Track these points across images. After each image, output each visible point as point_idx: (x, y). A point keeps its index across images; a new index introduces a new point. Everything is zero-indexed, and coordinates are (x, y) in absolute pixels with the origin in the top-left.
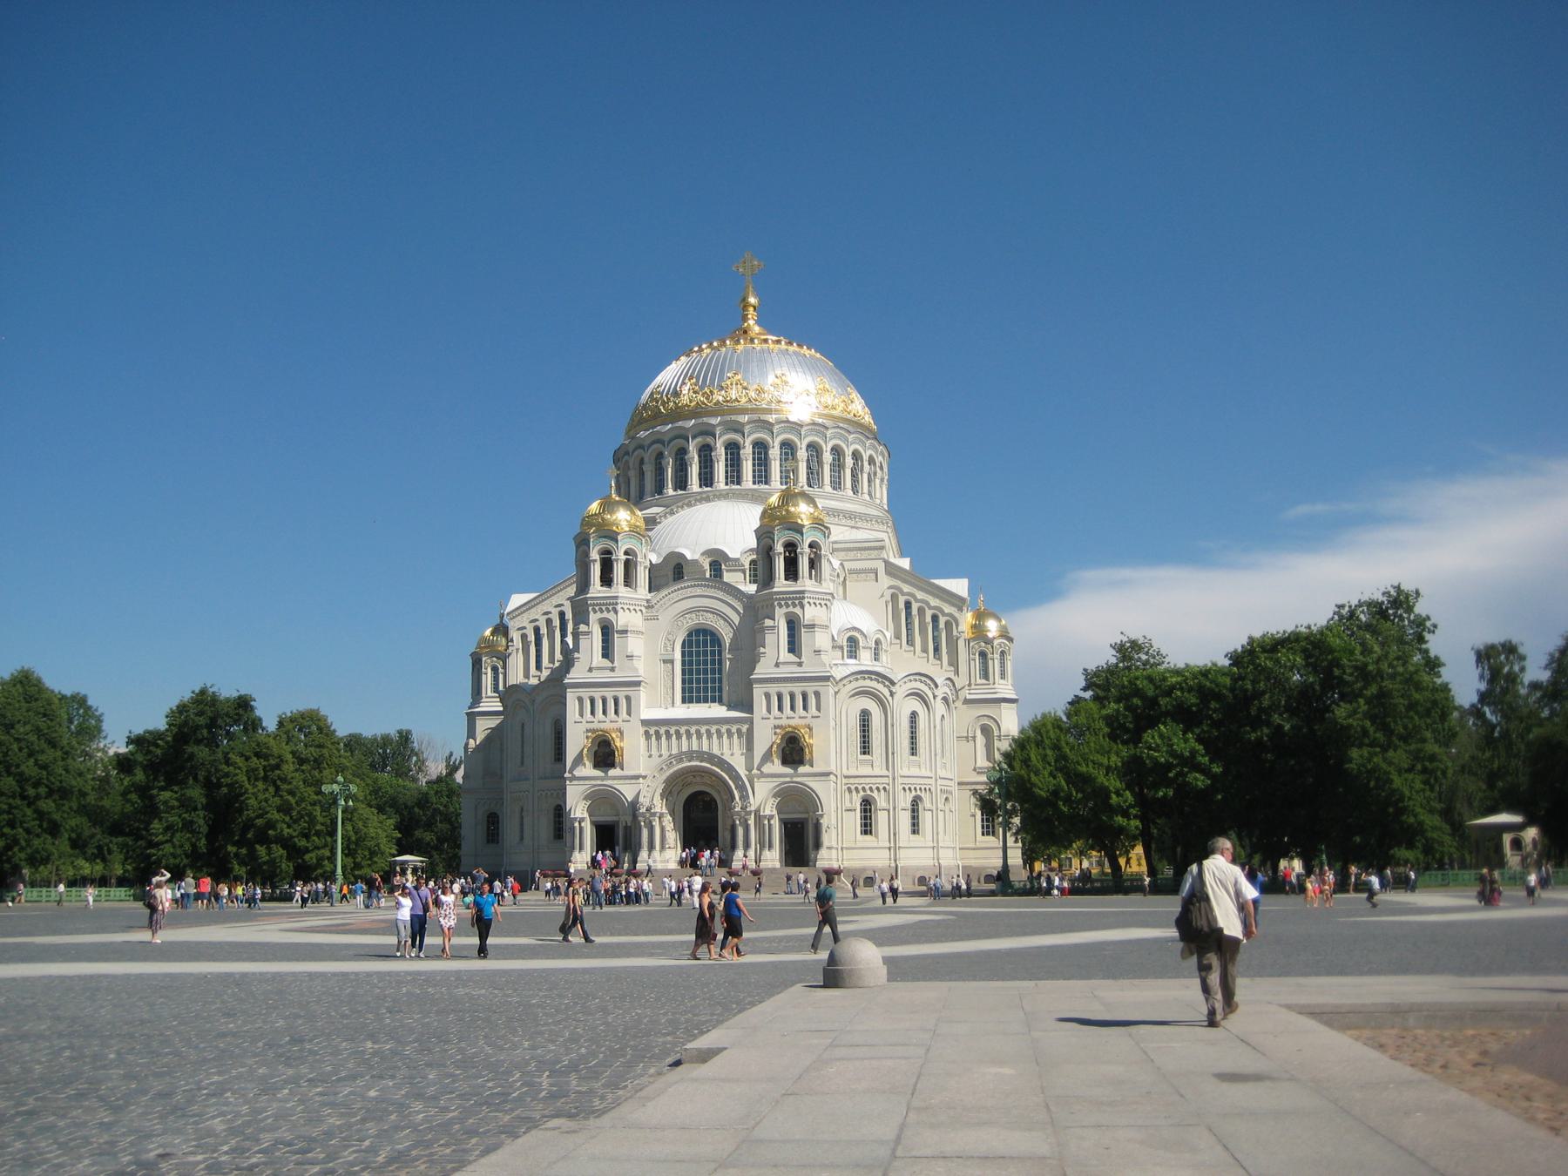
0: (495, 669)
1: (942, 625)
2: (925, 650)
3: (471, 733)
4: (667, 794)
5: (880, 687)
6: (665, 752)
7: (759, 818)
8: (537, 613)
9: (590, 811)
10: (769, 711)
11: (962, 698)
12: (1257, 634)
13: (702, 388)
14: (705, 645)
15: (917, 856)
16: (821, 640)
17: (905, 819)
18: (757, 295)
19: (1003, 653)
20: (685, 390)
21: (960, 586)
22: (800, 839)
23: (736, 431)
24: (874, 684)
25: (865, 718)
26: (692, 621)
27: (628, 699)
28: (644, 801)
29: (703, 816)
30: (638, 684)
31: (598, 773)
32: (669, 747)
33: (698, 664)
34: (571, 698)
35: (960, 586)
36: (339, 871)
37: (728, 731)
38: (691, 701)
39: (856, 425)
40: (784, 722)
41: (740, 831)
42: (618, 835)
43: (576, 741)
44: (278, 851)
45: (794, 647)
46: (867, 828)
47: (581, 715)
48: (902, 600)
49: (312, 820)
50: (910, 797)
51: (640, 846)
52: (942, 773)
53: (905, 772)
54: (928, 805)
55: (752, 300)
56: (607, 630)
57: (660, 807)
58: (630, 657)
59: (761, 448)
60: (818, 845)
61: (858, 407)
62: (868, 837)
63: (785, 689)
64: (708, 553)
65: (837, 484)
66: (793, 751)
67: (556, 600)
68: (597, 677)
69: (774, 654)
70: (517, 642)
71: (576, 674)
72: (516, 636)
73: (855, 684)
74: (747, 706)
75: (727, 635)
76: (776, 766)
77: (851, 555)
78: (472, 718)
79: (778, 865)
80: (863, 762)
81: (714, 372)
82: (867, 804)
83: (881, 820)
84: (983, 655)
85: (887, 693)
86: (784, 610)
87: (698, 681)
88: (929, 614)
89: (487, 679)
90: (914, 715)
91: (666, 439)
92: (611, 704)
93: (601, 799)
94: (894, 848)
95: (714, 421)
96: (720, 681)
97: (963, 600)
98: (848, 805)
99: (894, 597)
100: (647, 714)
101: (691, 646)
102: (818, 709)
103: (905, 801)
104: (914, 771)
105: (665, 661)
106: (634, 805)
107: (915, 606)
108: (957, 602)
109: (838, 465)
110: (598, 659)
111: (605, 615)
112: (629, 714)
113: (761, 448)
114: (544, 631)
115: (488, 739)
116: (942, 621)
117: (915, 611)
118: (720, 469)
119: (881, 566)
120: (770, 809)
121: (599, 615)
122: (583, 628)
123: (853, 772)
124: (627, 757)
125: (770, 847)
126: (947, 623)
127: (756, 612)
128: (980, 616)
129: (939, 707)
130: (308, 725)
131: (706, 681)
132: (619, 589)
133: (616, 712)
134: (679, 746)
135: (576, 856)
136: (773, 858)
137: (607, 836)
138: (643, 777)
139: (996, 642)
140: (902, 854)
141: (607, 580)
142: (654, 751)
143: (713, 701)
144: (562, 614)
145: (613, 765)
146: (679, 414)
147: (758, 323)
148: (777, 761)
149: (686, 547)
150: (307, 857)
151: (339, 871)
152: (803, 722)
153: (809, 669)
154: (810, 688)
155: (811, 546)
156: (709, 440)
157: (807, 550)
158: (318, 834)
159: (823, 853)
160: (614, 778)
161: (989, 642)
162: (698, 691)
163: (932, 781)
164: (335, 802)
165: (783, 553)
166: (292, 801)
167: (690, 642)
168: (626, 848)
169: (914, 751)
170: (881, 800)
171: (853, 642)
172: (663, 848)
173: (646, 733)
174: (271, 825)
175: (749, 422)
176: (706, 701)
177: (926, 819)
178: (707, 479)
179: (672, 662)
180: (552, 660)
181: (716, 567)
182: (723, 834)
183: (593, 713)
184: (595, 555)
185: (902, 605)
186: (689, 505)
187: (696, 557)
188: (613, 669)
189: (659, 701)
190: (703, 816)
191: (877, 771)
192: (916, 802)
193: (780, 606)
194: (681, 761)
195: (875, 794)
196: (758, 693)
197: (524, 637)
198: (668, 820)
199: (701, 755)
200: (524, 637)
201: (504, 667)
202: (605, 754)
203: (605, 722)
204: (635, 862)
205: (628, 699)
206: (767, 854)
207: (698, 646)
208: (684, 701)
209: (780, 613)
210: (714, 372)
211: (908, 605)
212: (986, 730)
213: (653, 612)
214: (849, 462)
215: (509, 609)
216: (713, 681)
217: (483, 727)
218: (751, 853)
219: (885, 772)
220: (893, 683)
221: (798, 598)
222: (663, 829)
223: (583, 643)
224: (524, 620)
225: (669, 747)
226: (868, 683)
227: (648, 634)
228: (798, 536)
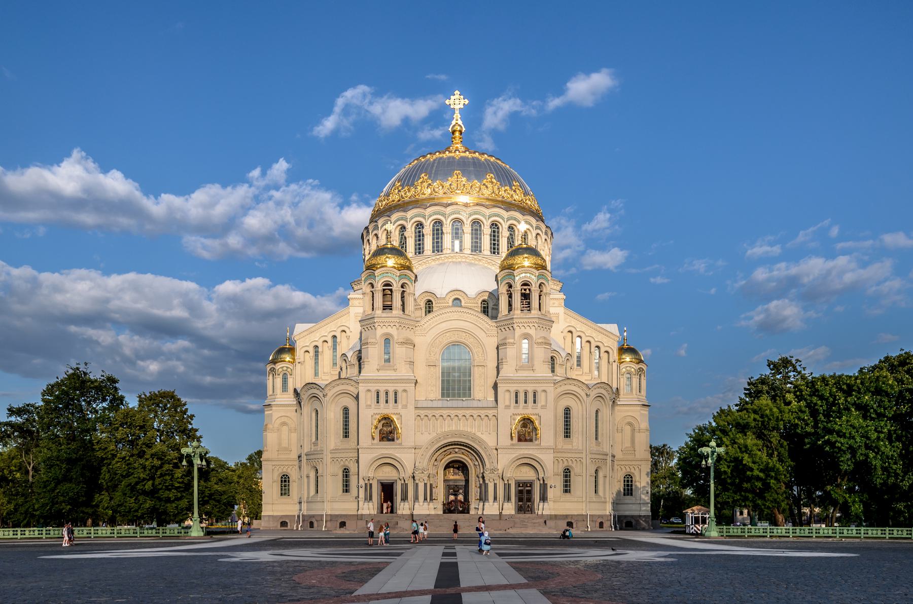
68: (383, 374)
79: (513, 512)
82: (567, 473)
125: (509, 499)
136: (510, 508)
170: (576, 470)
178: (438, 247)
182: (474, 492)
202: (388, 432)
206: (506, 505)
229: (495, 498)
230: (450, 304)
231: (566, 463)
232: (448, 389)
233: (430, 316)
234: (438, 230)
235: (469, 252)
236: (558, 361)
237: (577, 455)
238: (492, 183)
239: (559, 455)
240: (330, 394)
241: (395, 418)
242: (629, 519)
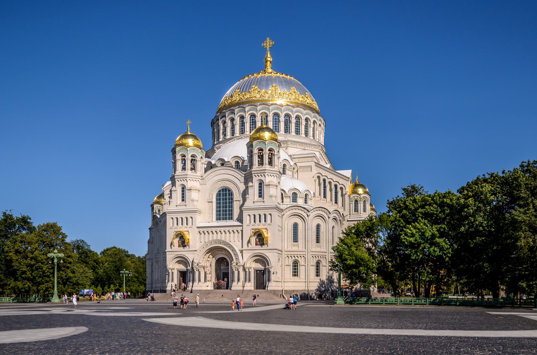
5: (302, 213)
11: (346, 220)
13: (241, 93)
16: (272, 191)
17: (313, 270)
18: (272, 56)
19: (365, 202)
22: (262, 278)
24: (300, 212)
25: (296, 226)
30: (195, 212)
34: (168, 217)
35: (348, 173)
38: (220, 219)
46: (295, 273)
50: (315, 261)
53: (314, 250)
54: (324, 264)
55: (269, 59)
58: (192, 200)
61: (309, 100)
62: (296, 277)
65: (298, 132)
77: (301, 160)
79: (252, 288)
80: (293, 245)
81: (247, 85)
82: (296, 264)
83: (302, 270)
85: (305, 215)
86: (258, 178)
90: (318, 226)
92: (185, 220)
98: (287, 263)
103: (314, 262)
109: (298, 124)
110: (179, 201)
119: (313, 164)
121: (181, 183)
123: (290, 249)
124: (191, 243)
125: (249, 281)
129: (331, 223)
130: (53, 229)
136: (250, 286)
137: (184, 276)
142: (202, 240)
149: (225, 156)
152: (265, 227)
157: (268, 152)
169: (318, 241)
170: (301, 261)
171: (295, 195)
172: (205, 281)
195: (299, 259)
206: (247, 284)
208: (217, 220)
210: (247, 85)
214: (304, 123)
218: (240, 283)
219: (304, 250)
221: (263, 173)
229: (239, 280)
231: (293, 258)
232: (220, 215)
234: (253, 120)
235: (283, 133)
236: (309, 197)
237: (323, 254)
238: (295, 92)
239: (289, 253)
241: (186, 233)
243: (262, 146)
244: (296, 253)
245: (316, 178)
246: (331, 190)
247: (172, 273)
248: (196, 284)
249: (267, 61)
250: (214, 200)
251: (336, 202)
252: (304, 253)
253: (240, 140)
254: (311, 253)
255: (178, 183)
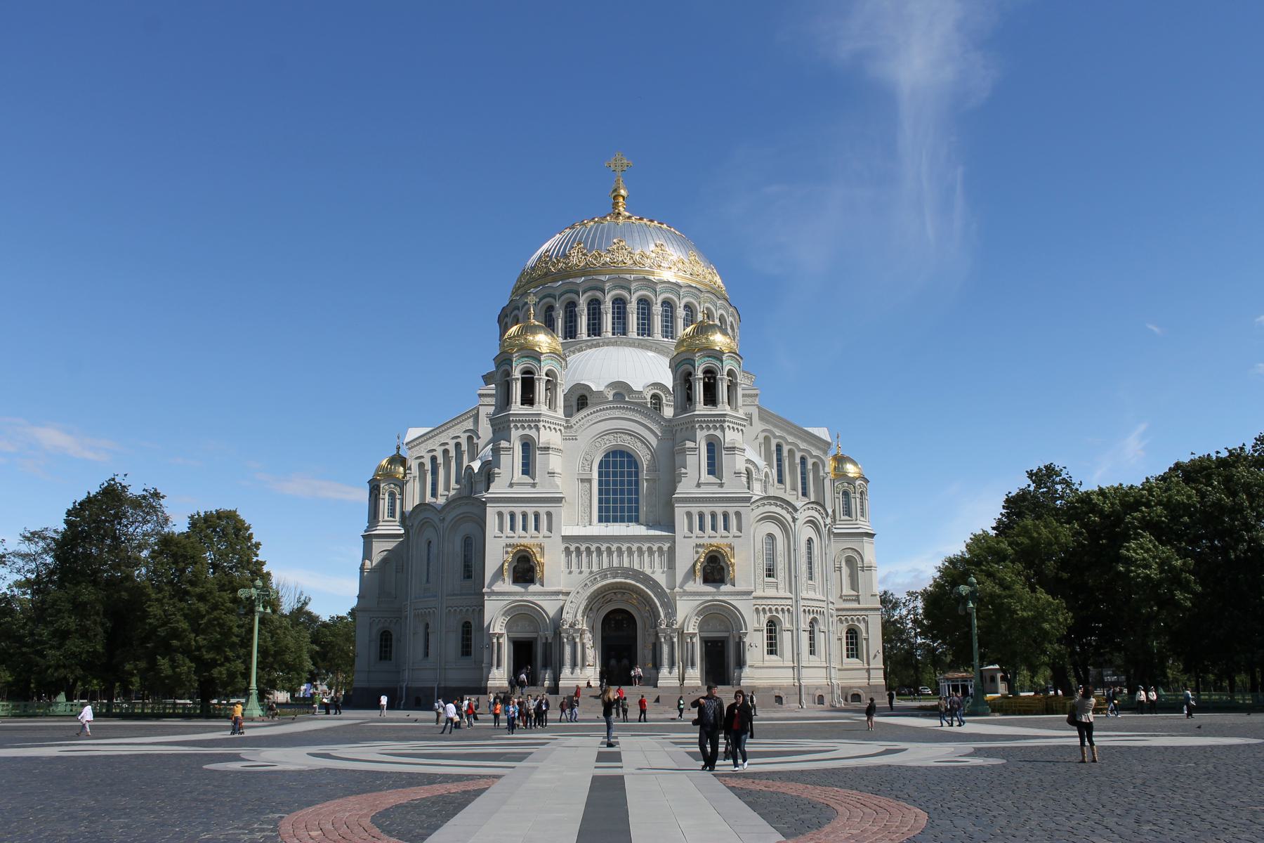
0: (392, 495)
1: (810, 466)
2: (794, 489)
3: (367, 554)
4: (589, 609)
5: (784, 513)
6: (595, 569)
7: (681, 633)
8: (434, 444)
9: (509, 626)
10: (691, 530)
12: (1186, 459)
13: (590, 251)
14: (622, 466)
15: (814, 677)
19: (862, 493)
20: (574, 252)
21: (823, 433)
23: (623, 288)
24: (778, 510)
26: (611, 442)
27: (549, 515)
28: (568, 617)
29: (625, 635)
30: (559, 500)
31: (517, 588)
32: (590, 565)
33: (615, 483)
34: (491, 513)
36: (254, 685)
37: (650, 549)
38: (607, 521)
39: (714, 292)
40: (706, 541)
41: (665, 649)
42: (535, 653)
43: (496, 554)
44: (186, 666)
45: (714, 467)
47: (501, 530)
48: (774, 442)
49: (227, 633)
51: (561, 664)
52: (831, 599)
53: (804, 595)
55: (623, 192)
56: (528, 447)
57: (583, 625)
58: (552, 474)
59: (644, 304)
60: (740, 664)
62: (773, 657)
63: (707, 509)
64: (614, 385)
66: (715, 569)
67: (452, 432)
69: (693, 477)
70: (415, 471)
71: (498, 488)
72: (414, 465)
73: (762, 509)
74: (671, 527)
75: (644, 457)
76: (698, 585)
78: (368, 539)
80: (769, 585)
82: (772, 624)
83: (786, 640)
84: (846, 494)
86: (705, 432)
87: (615, 501)
88: (798, 456)
89: (384, 505)
90: (810, 541)
91: (557, 293)
93: (522, 614)
94: (797, 668)
95: (602, 278)
96: (637, 501)
97: (829, 444)
99: (767, 439)
100: (568, 531)
101: (607, 466)
102: (740, 529)
103: (804, 625)
104: (811, 595)
105: (582, 481)
106: (557, 622)
107: (785, 449)
108: (824, 445)
111: (527, 432)
112: (550, 529)
113: (644, 304)
114: (440, 460)
115: (384, 561)
116: (810, 462)
117: (785, 453)
118: (608, 321)
120: (692, 628)
121: (521, 432)
122: (504, 444)
123: (759, 593)
125: (693, 665)
126: (814, 464)
127: (675, 439)
128: (840, 460)
131: (622, 501)
132: (541, 407)
133: (537, 528)
134: (600, 563)
135: (495, 673)
136: (695, 676)
137: (524, 654)
138: (565, 590)
139: (858, 482)
140: (804, 672)
141: (528, 399)
143: (630, 520)
144: (458, 445)
145: (532, 581)
146: (567, 273)
147: (626, 210)
148: (699, 579)
150: (215, 672)
151: (254, 685)
152: (725, 541)
153: (733, 487)
154: (731, 509)
155: (729, 375)
156: (599, 294)
158: (232, 646)
159: (747, 671)
160: (535, 594)
161: (851, 481)
162: (615, 510)
163: (824, 604)
164: (251, 611)
165: (698, 382)
166: (202, 607)
167: (607, 463)
168: (545, 666)
173: (567, 549)
174: (176, 634)
175: (636, 280)
176: (622, 521)
177: (820, 639)
178: (595, 329)
179: (589, 481)
180: (447, 488)
181: (619, 397)
183: (512, 528)
184: (517, 374)
185: (774, 448)
186: (580, 350)
187: (601, 389)
188: (534, 485)
189: (578, 518)
190: (625, 635)
191: (782, 593)
192: (813, 622)
193: (702, 428)
194: (605, 577)
195: (780, 615)
196: (680, 512)
197: (421, 465)
198: (588, 635)
199: (628, 572)
200: (421, 465)
201: (402, 493)
202: (525, 569)
203: (527, 538)
204: (556, 679)
205: (549, 515)
207: (615, 466)
208: (600, 520)
209: (701, 435)
211: (779, 447)
212: (850, 561)
213: (570, 433)
215: (407, 440)
216: (630, 501)
217: (380, 549)
219: (788, 595)
220: (796, 510)
221: (720, 420)
222: (583, 645)
223: (505, 459)
224: (422, 450)
225: (590, 565)
226: (773, 508)
227: (570, 456)
228: (718, 363)
230: (611, 398)
231: (769, 614)
232: (607, 510)
233: (583, 413)
239: (759, 602)
240: (449, 519)
242: (855, 691)
243: (713, 363)
244: (774, 602)
245: (761, 439)
246: (792, 465)
247: (499, 644)
248: (578, 670)
249: (615, 198)
250: (595, 475)
251: (804, 494)
252: (789, 602)
253: (611, 348)
254: (802, 603)
255: (516, 434)
